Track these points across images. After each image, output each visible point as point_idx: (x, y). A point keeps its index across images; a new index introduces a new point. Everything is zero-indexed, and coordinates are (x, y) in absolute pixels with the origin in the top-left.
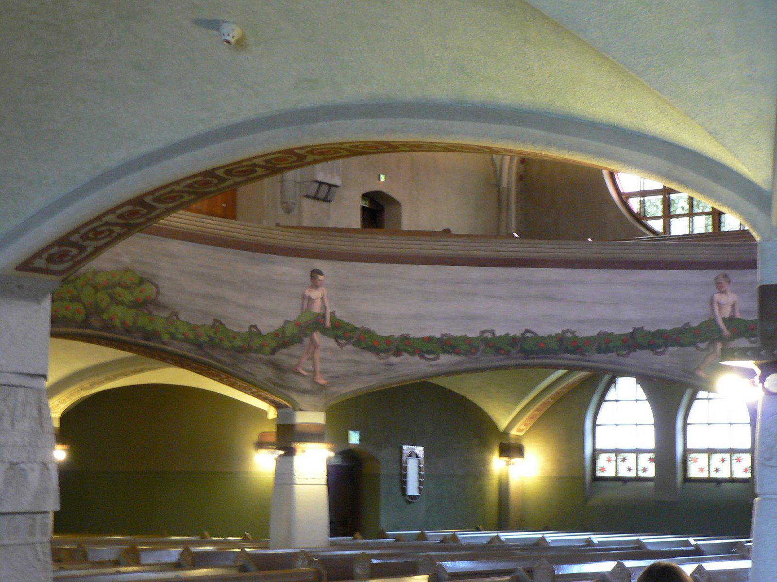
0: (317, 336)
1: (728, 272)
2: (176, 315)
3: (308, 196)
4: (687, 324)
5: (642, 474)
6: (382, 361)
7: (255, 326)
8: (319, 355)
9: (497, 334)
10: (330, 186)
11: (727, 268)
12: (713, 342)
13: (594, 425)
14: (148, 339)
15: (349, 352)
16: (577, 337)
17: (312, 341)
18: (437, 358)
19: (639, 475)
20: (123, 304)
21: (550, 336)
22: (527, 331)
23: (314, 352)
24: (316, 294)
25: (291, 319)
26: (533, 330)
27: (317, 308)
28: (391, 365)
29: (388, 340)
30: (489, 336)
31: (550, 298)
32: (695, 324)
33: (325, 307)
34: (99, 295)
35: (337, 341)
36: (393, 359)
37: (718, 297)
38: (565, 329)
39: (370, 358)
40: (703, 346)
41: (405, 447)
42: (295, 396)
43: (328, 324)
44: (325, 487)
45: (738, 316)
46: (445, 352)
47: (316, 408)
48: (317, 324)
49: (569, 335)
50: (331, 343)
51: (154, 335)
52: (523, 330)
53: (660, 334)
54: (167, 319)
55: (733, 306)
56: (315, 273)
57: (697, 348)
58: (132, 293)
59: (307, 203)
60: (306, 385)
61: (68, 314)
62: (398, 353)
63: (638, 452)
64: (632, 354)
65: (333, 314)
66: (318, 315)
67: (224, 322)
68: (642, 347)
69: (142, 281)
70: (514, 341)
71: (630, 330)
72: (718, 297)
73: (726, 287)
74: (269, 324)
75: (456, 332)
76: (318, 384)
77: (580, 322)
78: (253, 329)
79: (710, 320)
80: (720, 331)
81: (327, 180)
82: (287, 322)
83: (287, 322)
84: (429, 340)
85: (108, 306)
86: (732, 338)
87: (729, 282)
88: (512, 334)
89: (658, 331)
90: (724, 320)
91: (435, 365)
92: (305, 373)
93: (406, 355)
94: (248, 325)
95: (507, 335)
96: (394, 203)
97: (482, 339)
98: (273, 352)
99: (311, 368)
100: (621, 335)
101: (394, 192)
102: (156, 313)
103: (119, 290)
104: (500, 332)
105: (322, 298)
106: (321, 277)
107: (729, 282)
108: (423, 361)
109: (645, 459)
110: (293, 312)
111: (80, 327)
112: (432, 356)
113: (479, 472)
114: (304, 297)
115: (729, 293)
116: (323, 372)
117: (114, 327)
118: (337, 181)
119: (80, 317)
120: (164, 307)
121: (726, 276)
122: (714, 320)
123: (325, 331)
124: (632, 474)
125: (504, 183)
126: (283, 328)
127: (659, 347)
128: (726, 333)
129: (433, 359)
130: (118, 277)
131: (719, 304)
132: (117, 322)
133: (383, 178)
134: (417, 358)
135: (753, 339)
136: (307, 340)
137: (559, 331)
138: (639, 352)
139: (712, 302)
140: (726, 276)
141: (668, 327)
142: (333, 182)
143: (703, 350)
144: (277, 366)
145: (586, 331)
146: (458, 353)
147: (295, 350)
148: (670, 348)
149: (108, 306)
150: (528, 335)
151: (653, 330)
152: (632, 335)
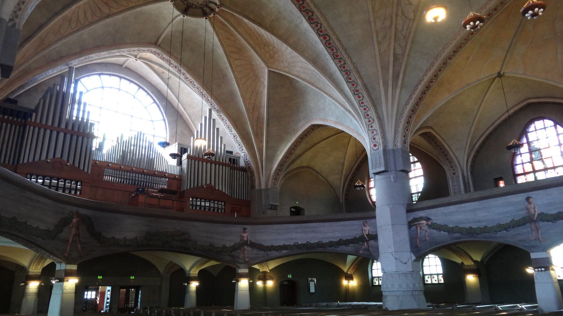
0: (245, 247)
1: (366, 220)
2: (196, 243)
3: (268, 209)
4: (356, 237)
5: (440, 282)
6: (265, 253)
7: (225, 245)
8: (246, 252)
9: (299, 243)
10: (276, 206)
11: (366, 219)
12: (363, 242)
13: (372, 270)
15: (255, 251)
16: (323, 243)
17: (244, 248)
18: (282, 251)
19: (433, 283)
21: (315, 243)
22: (308, 242)
23: (244, 252)
24: (245, 235)
25: (237, 242)
26: (309, 241)
27: (245, 239)
28: (268, 254)
29: (267, 247)
30: (296, 244)
31: (313, 232)
32: (358, 237)
33: (248, 239)
35: (252, 248)
36: (269, 252)
37: (364, 228)
38: (319, 241)
39: (262, 252)
40: (360, 243)
41: (309, 278)
42: (238, 265)
43: (249, 243)
44: (248, 291)
45: (370, 233)
46: (284, 249)
47: (245, 268)
48: (246, 243)
49: (320, 242)
50: (250, 249)
52: (306, 241)
53: (347, 240)
55: (369, 230)
56: (245, 229)
57: (359, 244)
59: (268, 210)
60: (241, 261)
62: (270, 251)
63: (438, 275)
64: (339, 247)
65: (250, 240)
66: (246, 241)
67: (213, 244)
68: (342, 245)
70: (303, 245)
71: (338, 240)
72: (364, 228)
73: (366, 225)
74: (229, 244)
75: (287, 243)
76: (245, 261)
77: (323, 238)
78: (224, 246)
79: (362, 235)
80: (366, 238)
81: (274, 204)
82: (235, 243)
83: (235, 243)
84: (280, 246)
86: (369, 240)
87: (367, 223)
88: (303, 243)
89: (347, 239)
90: (366, 235)
91: (281, 254)
92: (242, 258)
93: (272, 251)
94: (222, 245)
95: (302, 243)
96: (303, 209)
97: (295, 245)
98: (231, 252)
99: (243, 256)
100: (336, 242)
101: (301, 206)
104: (300, 243)
105: (247, 236)
106: (246, 230)
107: (367, 223)
108: (278, 253)
109: (441, 277)
110: (237, 240)
112: (280, 251)
113: (339, 285)
114: (241, 236)
115: (367, 227)
116: (248, 257)
118: (277, 204)
121: (366, 222)
122: (363, 235)
123: (248, 245)
124: (437, 282)
125: (341, 202)
126: (234, 245)
127: (347, 245)
128: (367, 239)
129: (280, 252)
131: (365, 230)
133: (297, 202)
134: (275, 252)
135: (375, 240)
136: (242, 248)
137: (317, 241)
138: (341, 246)
139: (362, 230)
140: (366, 222)
141: (350, 238)
142: (276, 204)
143: (361, 244)
144: (233, 257)
145: (325, 241)
146: (288, 250)
147: (239, 251)
148: (351, 245)
150: (308, 243)
151: (345, 239)
152: (338, 241)
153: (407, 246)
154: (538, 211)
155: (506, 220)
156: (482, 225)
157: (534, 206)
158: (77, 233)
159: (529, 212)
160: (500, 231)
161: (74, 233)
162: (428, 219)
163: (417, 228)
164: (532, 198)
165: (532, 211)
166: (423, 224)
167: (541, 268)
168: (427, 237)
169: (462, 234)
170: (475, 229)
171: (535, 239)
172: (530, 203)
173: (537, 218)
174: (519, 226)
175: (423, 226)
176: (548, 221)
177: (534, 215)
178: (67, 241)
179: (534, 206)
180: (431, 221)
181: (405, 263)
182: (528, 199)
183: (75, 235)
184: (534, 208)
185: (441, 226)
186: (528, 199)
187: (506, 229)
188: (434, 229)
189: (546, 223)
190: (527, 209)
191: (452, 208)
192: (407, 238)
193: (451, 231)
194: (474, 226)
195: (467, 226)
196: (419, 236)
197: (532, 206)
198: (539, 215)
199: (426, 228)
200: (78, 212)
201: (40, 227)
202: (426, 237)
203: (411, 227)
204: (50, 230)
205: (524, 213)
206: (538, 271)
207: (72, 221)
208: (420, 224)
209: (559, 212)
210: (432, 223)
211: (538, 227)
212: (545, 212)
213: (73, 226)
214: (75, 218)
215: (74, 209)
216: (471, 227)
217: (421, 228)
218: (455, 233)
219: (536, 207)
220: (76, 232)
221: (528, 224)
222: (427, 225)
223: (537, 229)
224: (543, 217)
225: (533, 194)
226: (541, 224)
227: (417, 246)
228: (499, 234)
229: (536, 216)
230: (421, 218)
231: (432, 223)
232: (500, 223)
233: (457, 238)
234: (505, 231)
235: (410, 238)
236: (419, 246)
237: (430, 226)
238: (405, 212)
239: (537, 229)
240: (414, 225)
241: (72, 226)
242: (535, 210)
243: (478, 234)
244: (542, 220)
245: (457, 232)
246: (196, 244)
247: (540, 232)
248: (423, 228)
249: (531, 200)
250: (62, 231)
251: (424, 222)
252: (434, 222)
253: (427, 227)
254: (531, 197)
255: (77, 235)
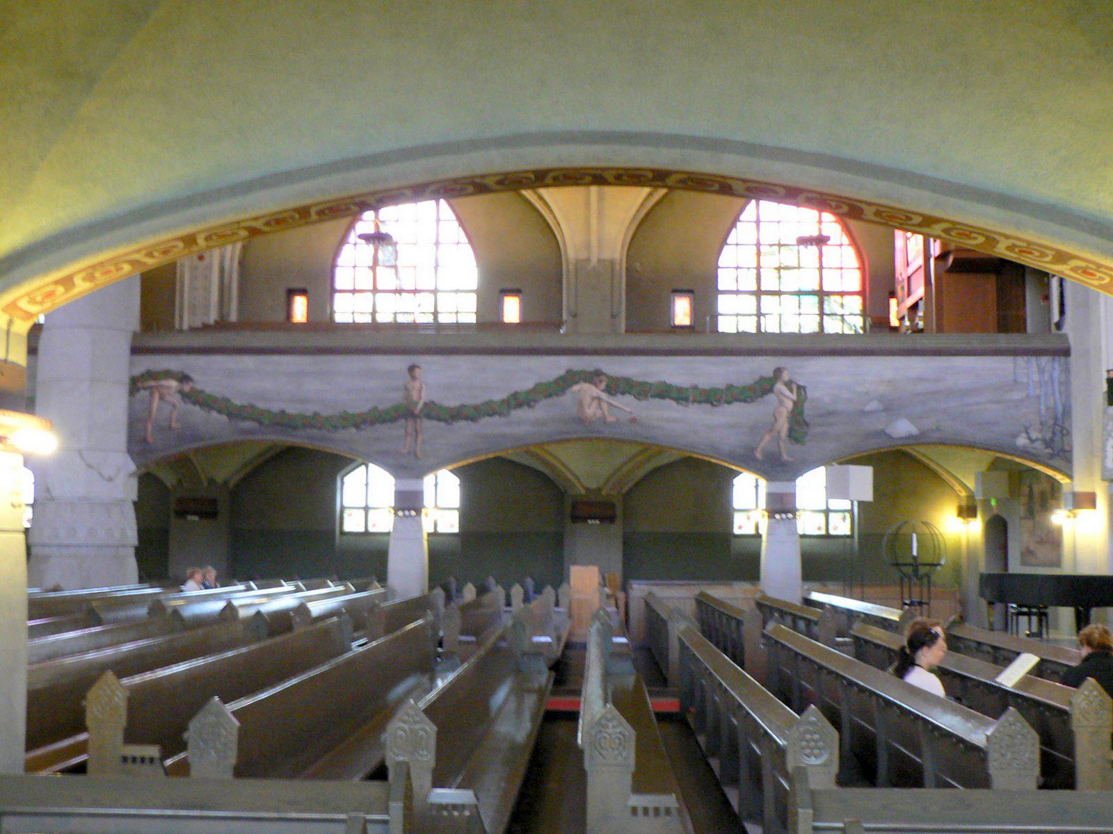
153: (121, 439)
154: (425, 397)
155: (360, 406)
156: (309, 410)
157: (421, 385)
159: (408, 397)
160: (344, 427)
162: (184, 378)
163: (152, 395)
164: (419, 367)
165: (415, 395)
166: (169, 387)
167: (409, 510)
168: (174, 420)
169: (260, 423)
170: (290, 417)
171: (409, 453)
172: (413, 377)
173: (421, 411)
174: (385, 421)
175: (169, 394)
176: (439, 419)
177: (417, 403)
179: (421, 385)
180: (191, 384)
181: (110, 479)
182: (412, 369)
184: (420, 391)
185: (215, 400)
186: (412, 369)
187: (357, 426)
188: (195, 403)
189: (435, 423)
190: (406, 389)
191: (248, 361)
192: (122, 419)
193: (235, 413)
194: (292, 409)
195: (275, 407)
196: (153, 415)
197: (417, 384)
198: (426, 404)
199: (176, 399)
202: (171, 421)
203: (138, 390)
205: (397, 397)
206: (405, 516)
208: (162, 386)
209: (463, 406)
210: (192, 388)
211: (419, 428)
212: (437, 400)
216: (283, 412)
217: (162, 398)
218: (244, 419)
219: (424, 386)
221: (402, 422)
222: (181, 392)
223: (416, 431)
224: (434, 412)
225: (423, 361)
226: (427, 423)
227: (145, 440)
228: (342, 434)
229: (420, 405)
230: (168, 374)
231: (192, 388)
232: (347, 410)
233: (249, 432)
234: (353, 430)
235: (130, 418)
236: (150, 440)
237: (186, 396)
238: (128, 351)
239: (416, 431)
240: (145, 389)
242: (420, 394)
243: (295, 428)
244: (429, 417)
245: (253, 420)
247: (420, 437)
248: (169, 398)
249: (417, 371)
251: (174, 384)
252: (199, 387)
253: (178, 397)
254: (419, 365)
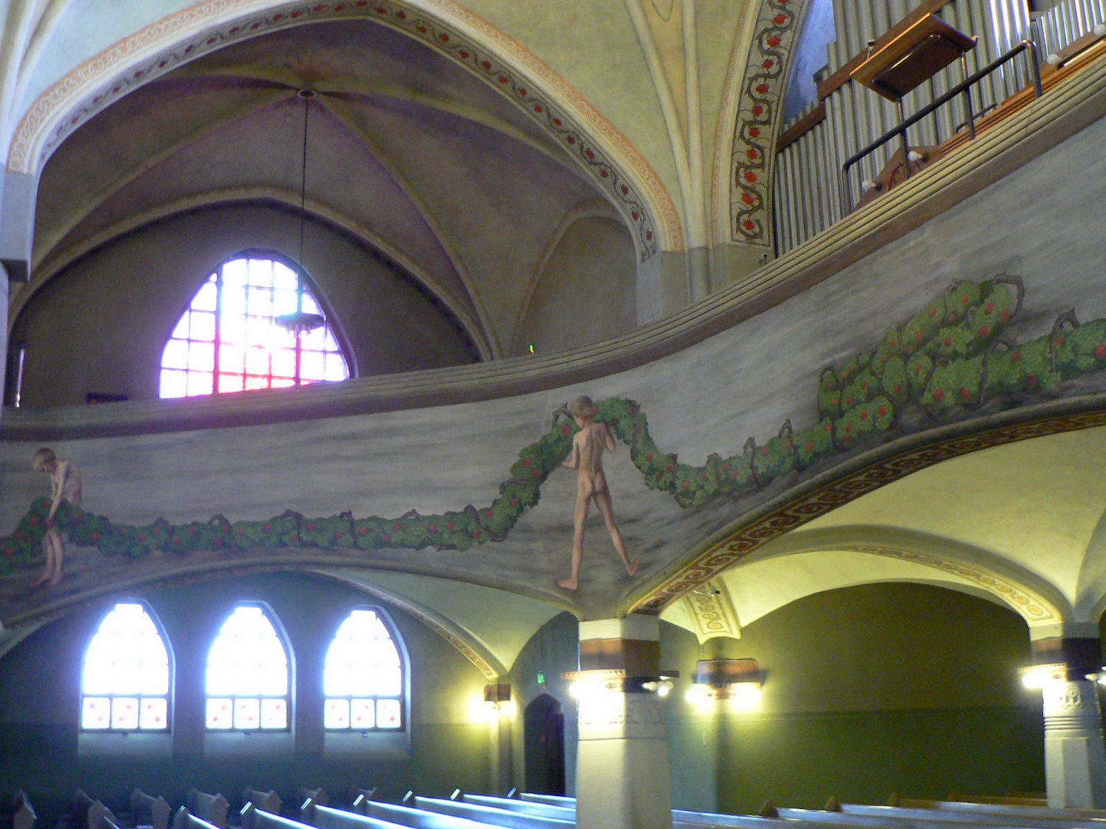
14: (1013, 405)
20: (955, 356)
34: (912, 365)
51: (1031, 387)
54: (1050, 338)
58: (968, 326)
61: (866, 426)
69: (986, 289)
85: (930, 374)
102: (1021, 340)
103: (945, 333)
111: (888, 440)
117: (944, 411)
119: (884, 423)
120: (1039, 316)
130: (941, 311)
132: (949, 399)
149: (930, 374)
158: (598, 488)
161: (588, 488)
178: (567, 529)
183: (594, 495)
200: (587, 401)
201: (423, 512)
204: (478, 507)
207: (569, 448)
213: (577, 466)
214: (579, 429)
215: (569, 395)
220: (593, 483)
241: (572, 464)
246: (1068, 327)
250: (537, 496)
255: (601, 493)
